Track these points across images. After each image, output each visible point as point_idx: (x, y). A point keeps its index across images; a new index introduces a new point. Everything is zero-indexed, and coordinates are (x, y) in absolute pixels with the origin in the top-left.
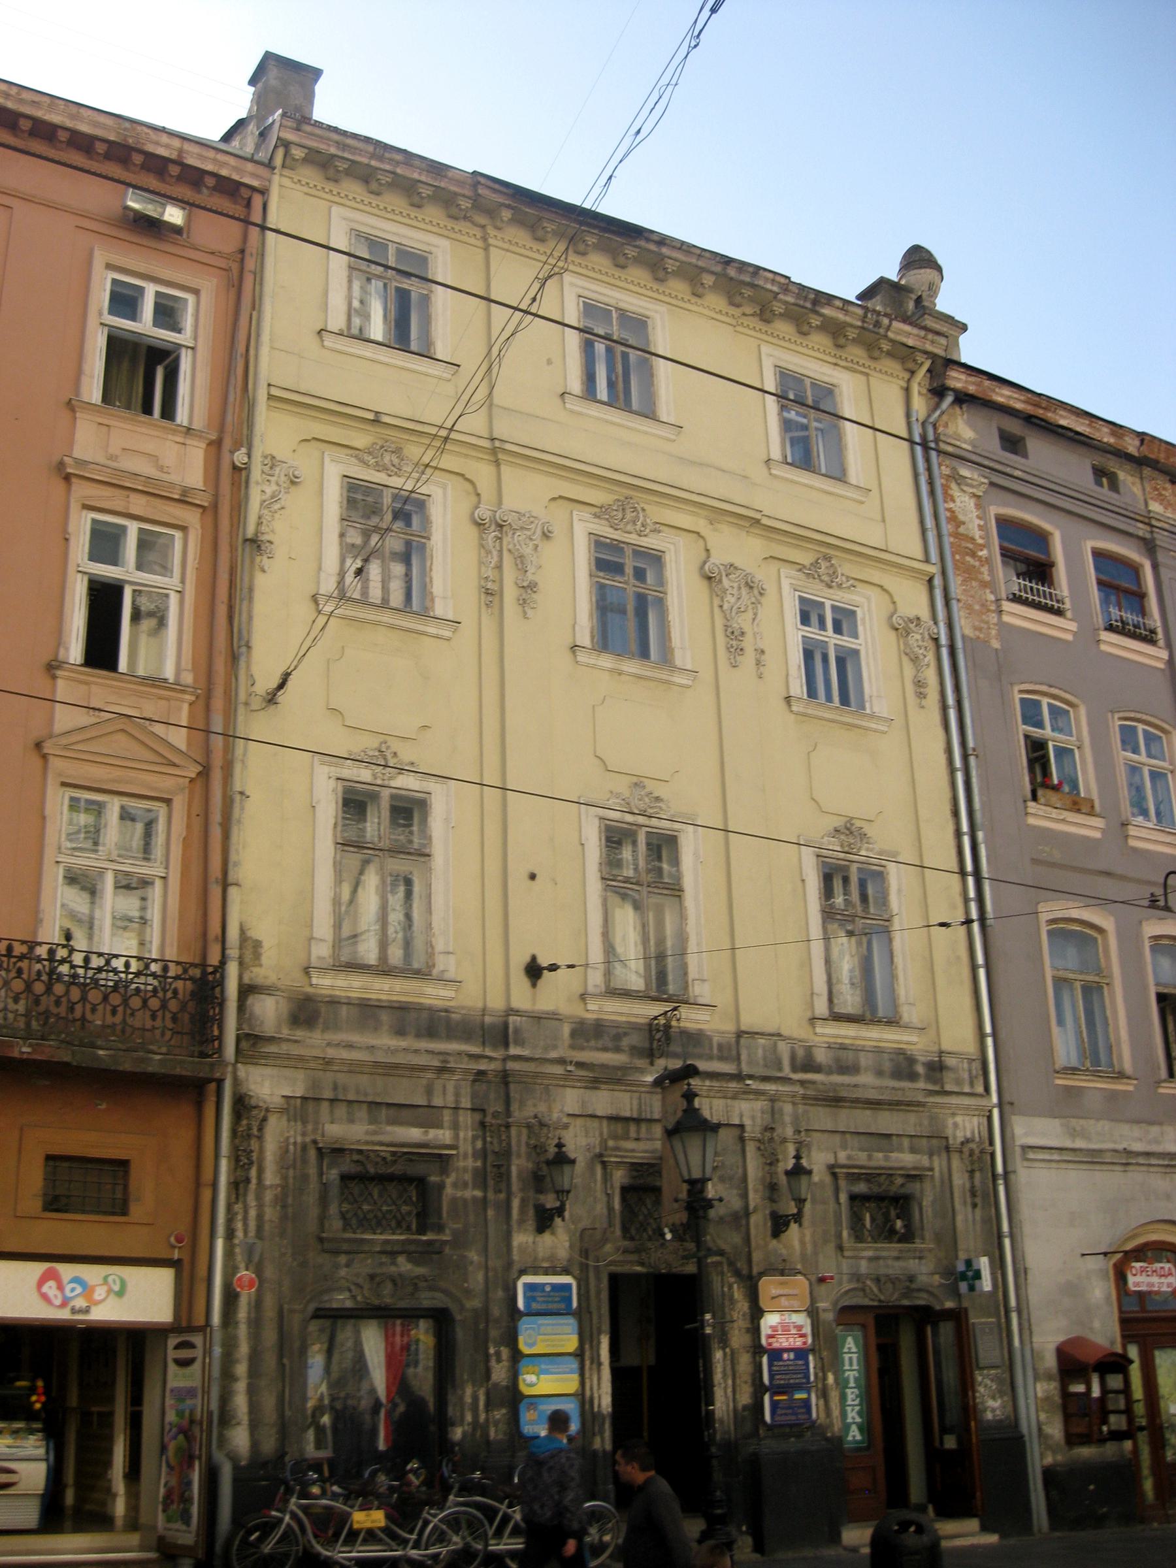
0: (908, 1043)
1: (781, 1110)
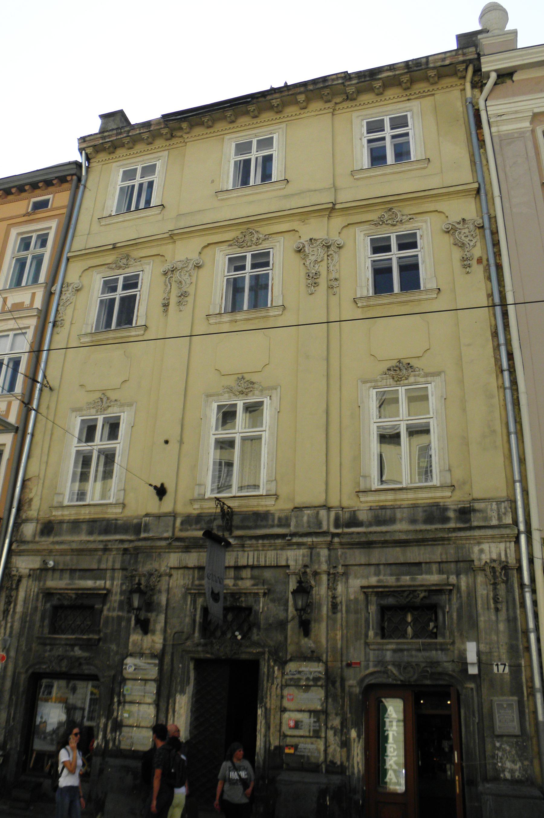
0: (442, 498)
1: (318, 555)
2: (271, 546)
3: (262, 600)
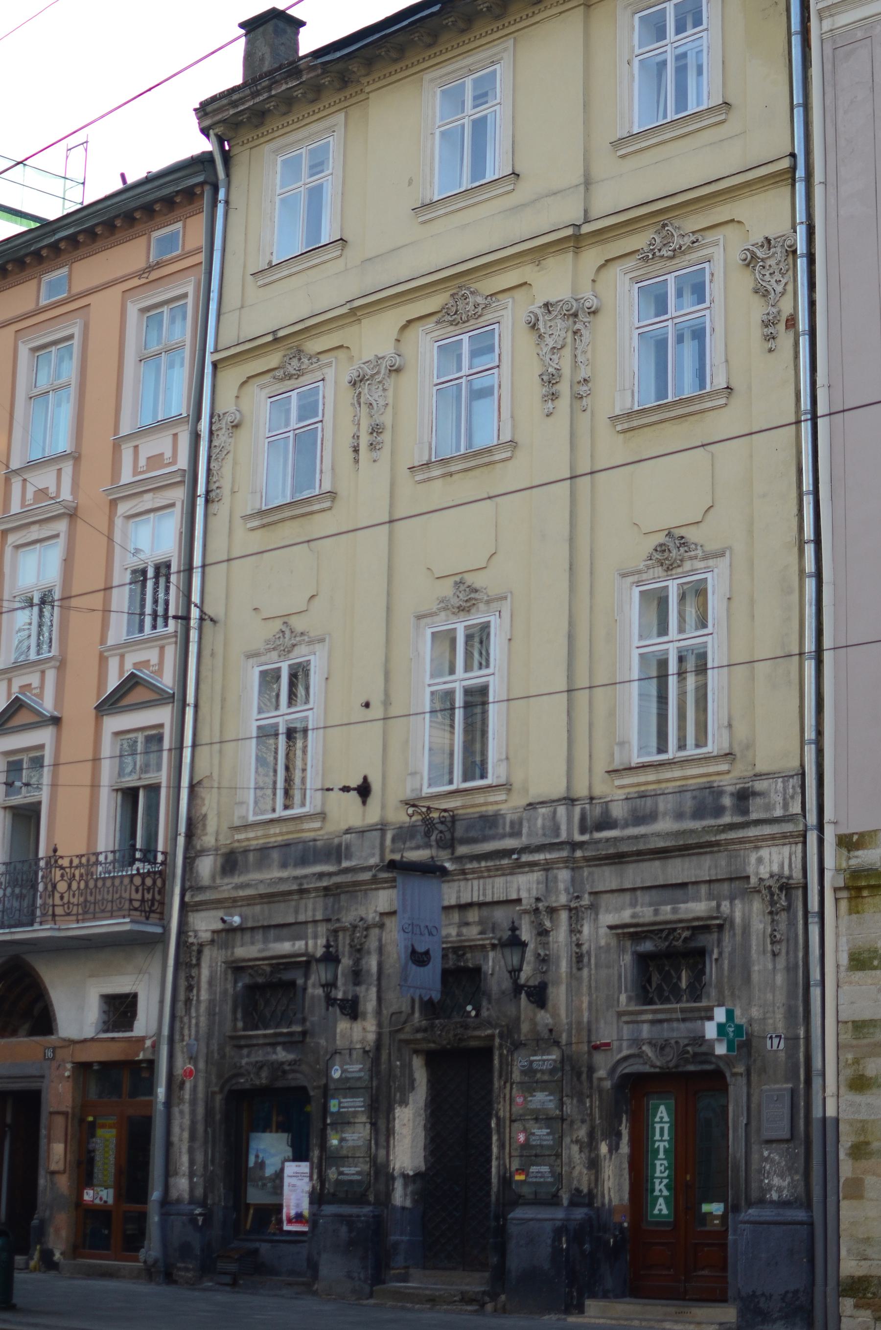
1: (556, 878)
2: (497, 870)
3: (491, 955)
